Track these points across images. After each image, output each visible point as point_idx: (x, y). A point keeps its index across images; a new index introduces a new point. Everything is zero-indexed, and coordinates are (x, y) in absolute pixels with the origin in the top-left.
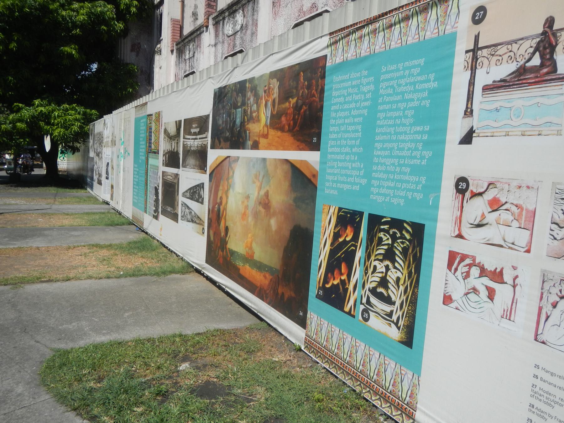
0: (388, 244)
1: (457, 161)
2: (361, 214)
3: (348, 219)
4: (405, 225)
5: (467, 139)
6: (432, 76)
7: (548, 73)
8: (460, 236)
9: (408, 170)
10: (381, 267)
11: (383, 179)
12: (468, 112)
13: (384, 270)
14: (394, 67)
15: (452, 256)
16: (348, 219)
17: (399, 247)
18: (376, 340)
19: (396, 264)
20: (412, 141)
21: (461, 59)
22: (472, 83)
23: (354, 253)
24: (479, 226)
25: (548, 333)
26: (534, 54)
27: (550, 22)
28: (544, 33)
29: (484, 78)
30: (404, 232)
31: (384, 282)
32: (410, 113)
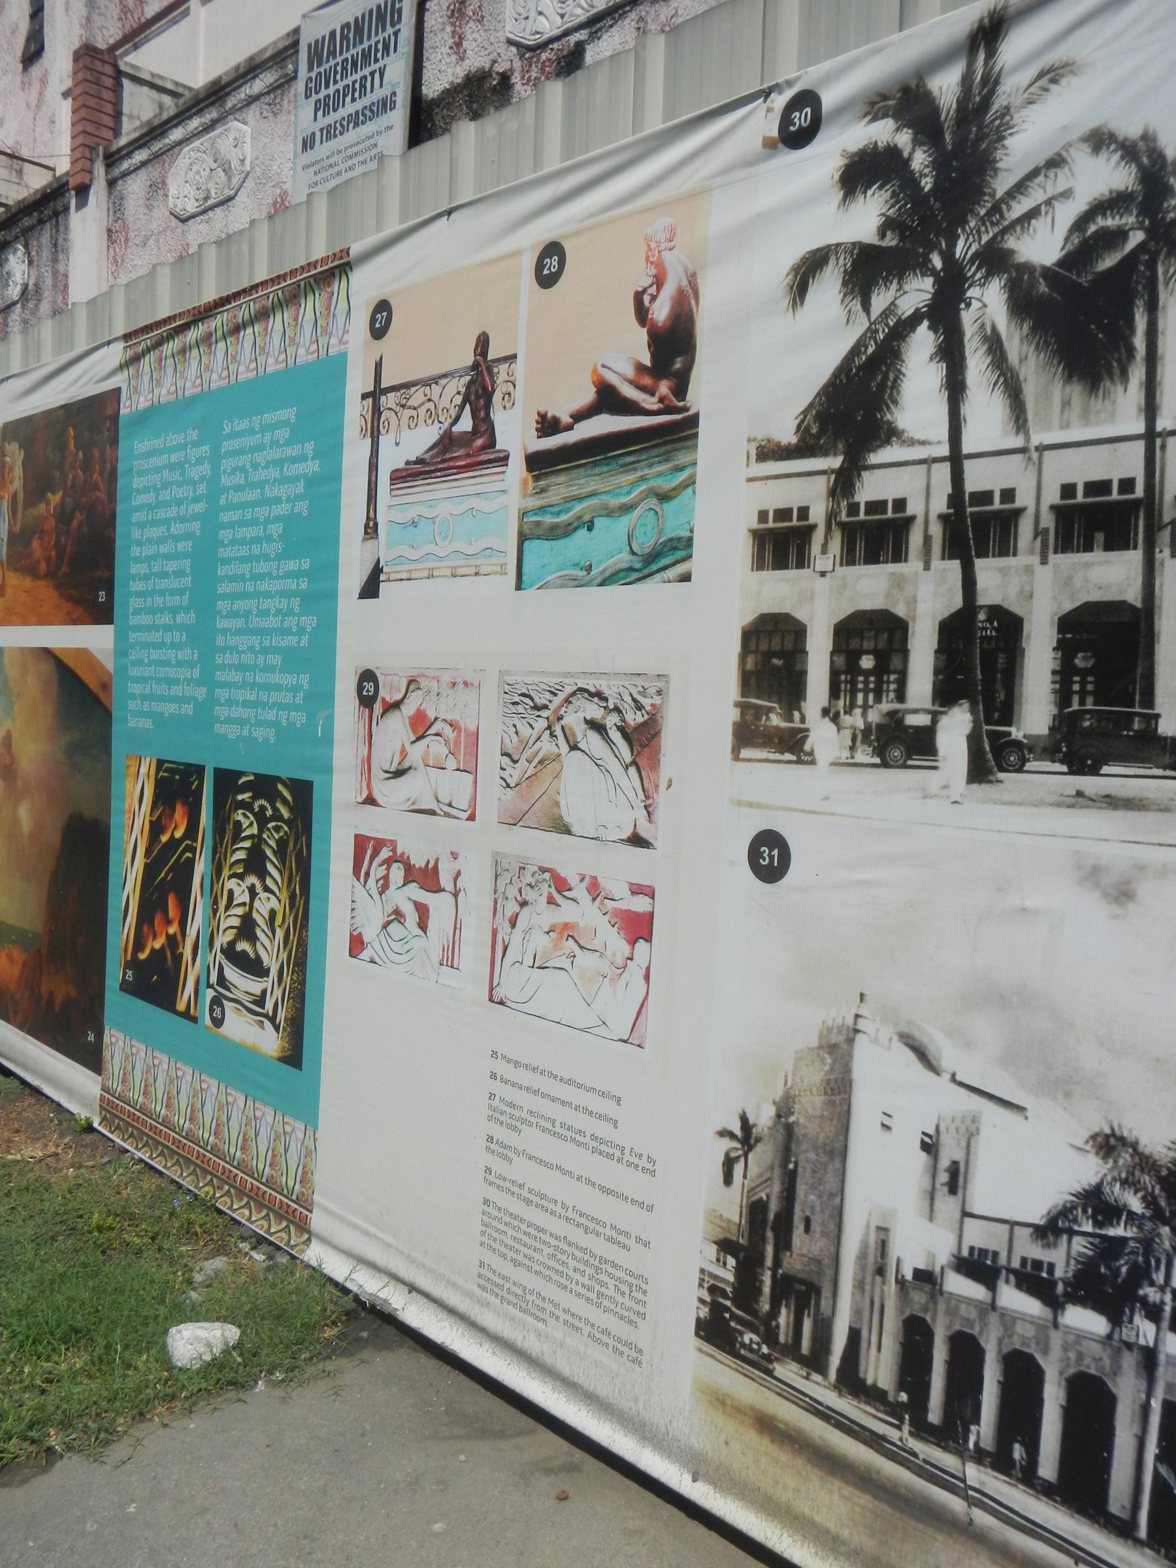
0: (251, 837)
2: (200, 770)
4: (280, 787)
6: (309, 447)
7: (483, 448)
8: (370, 801)
9: (275, 660)
11: (235, 685)
12: (371, 530)
13: (246, 898)
14: (243, 425)
16: (175, 786)
18: (234, 1065)
19: (269, 881)
20: (282, 594)
21: (355, 412)
22: (373, 466)
24: (399, 773)
26: (462, 407)
27: (483, 343)
28: (475, 366)
29: (392, 458)
30: (279, 805)
32: (276, 529)
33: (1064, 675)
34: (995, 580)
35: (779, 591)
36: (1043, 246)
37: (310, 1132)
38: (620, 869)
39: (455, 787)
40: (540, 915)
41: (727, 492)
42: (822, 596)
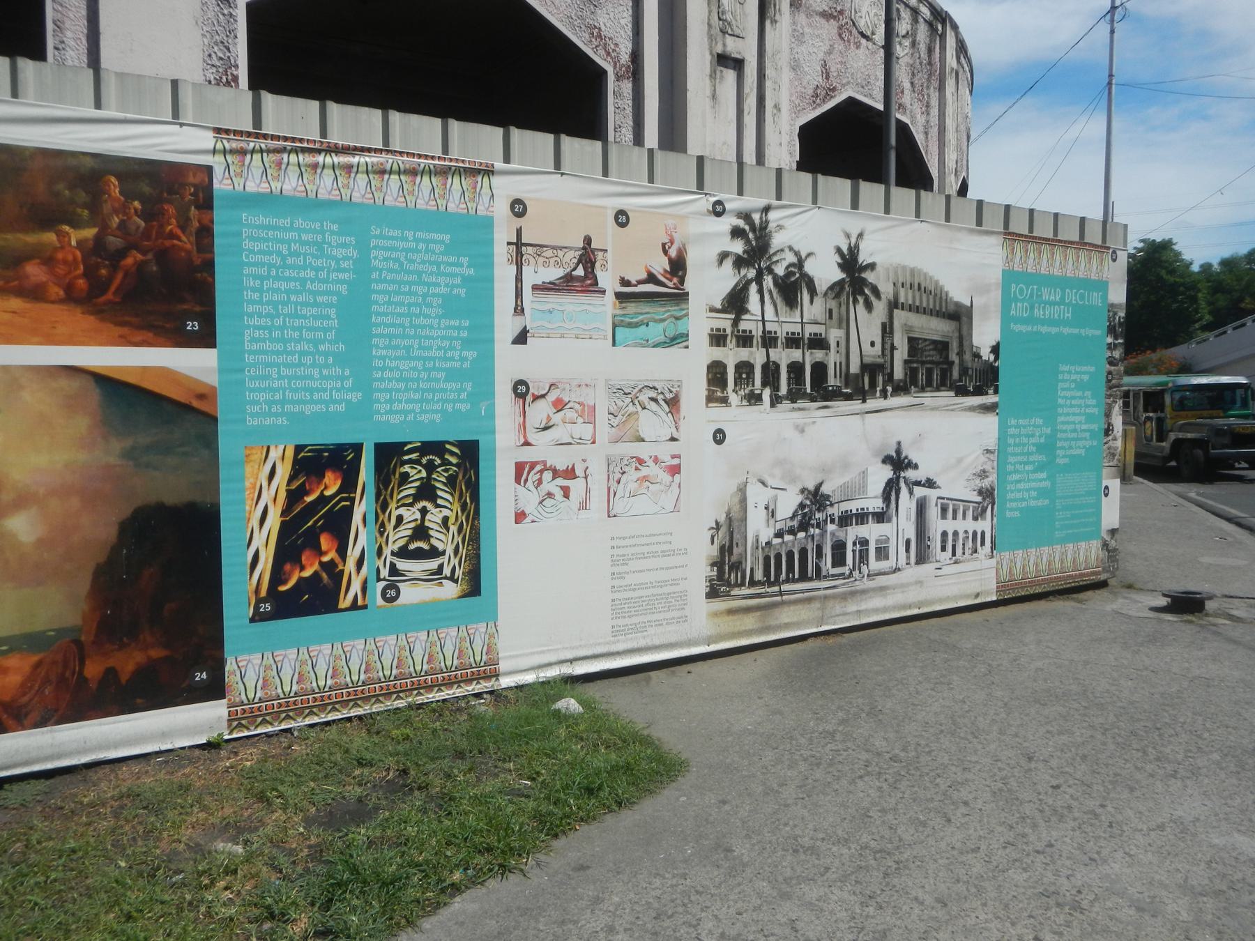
0: (422, 479)
1: (509, 363)
2: (358, 448)
3: (310, 463)
4: (448, 446)
5: (521, 338)
6: (465, 261)
7: (591, 285)
8: (527, 444)
9: (442, 375)
10: (411, 515)
11: (398, 391)
12: (519, 310)
13: (418, 516)
14: (397, 233)
15: (520, 468)
17: (440, 478)
19: (440, 501)
20: (443, 338)
21: (501, 252)
22: (519, 279)
23: (349, 511)
24: (546, 428)
25: (618, 507)
26: (578, 265)
27: (588, 240)
28: (584, 248)
29: (531, 277)
30: (447, 456)
31: (421, 532)
32: (437, 301)
33: (789, 378)
34: (775, 354)
35: (718, 354)
36: (780, 270)
37: (491, 624)
38: (665, 452)
39: (585, 431)
40: (632, 475)
41: (700, 319)
42: (731, 356)
